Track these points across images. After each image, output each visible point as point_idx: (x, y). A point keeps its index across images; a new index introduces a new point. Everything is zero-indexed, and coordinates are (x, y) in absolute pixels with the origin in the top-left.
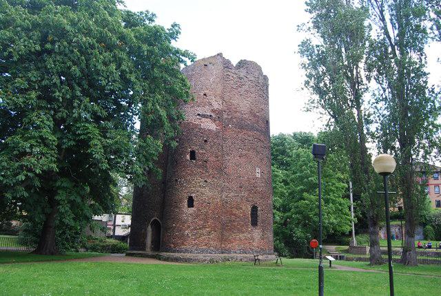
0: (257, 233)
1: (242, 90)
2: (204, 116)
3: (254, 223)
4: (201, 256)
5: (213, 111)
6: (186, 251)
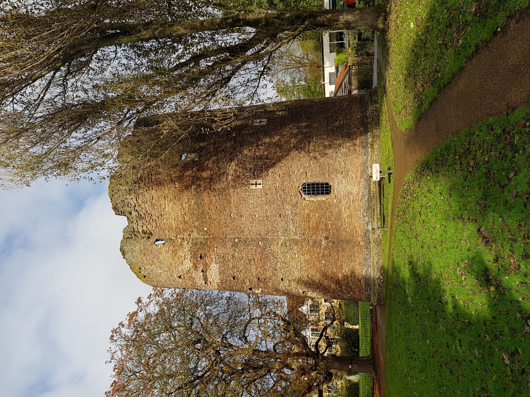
0: (340, 186)
2: (206, 279)
3: (324, 189)
5: (196, 268)
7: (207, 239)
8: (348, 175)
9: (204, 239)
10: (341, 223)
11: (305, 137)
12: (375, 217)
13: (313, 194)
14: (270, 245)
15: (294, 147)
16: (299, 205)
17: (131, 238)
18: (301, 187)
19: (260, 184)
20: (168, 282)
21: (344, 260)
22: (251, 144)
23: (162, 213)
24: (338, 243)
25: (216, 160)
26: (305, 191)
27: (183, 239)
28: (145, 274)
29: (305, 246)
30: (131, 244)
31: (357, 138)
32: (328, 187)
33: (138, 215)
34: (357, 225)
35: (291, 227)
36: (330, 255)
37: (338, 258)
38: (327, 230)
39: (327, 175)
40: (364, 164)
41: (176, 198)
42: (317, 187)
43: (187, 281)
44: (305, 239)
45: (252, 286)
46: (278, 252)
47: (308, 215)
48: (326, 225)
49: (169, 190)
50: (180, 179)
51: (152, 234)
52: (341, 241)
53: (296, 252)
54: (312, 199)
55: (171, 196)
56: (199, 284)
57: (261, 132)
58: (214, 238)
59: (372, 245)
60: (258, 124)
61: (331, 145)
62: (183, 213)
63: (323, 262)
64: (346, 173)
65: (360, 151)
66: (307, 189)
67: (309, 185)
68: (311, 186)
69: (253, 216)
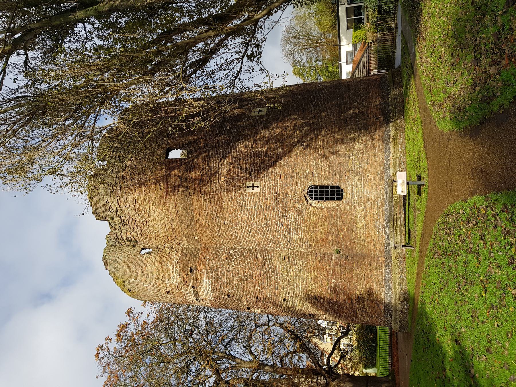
1: (140, 220)
2: (197, 295)
3: (334, 193)
5: (185, 283)
7: (199, 249)
8: (364, 176)
9: (195, 249)
10: (356, 234)
11: (313, 130)
12: (398, 229)
13: (322, 199)
14: (271, 259)
15: (299, 142)
16: (304, 212)
17: (116, 246)
18: (306, 191)
19: (258, 187)
20: (155, 297)
21: (359, 280)
22: (249, 136)
23: (147, 219)
24: (352, 258)
25: (207, 157)
26: (310, 195)
27: (172, 248)
28: (130, 287)
29: (311, 261)
30: (115, 253)
31: (376, 131)
32: (339, 191)
33: (120, 221)
34: (375, 237)
35: (295, 237)
36: (341, 273)
37: (352, 277)
38: (338, 242)
39: (338, 176)
40: (384, 163)
41: (162, 202)
42: (326, 191)
43: (176, 297)
44: (311, 252)
45: (249, 306)
46: (279, 268)
47: (315, 224)
48: (336, 236)
49: (154, 192)
50: (166, 179)
51: (137, 242)
52: (356, 256)
53: (301, 268)
54: (320, 205)
55: (156, 200)
56: (190, 300)
57: (259, 124)
58: (207, 248)
59: (394, 261)
60: (257, 114)
61: (343, 139)
62: (170, 219)
63: (333, 281)
64: (361, 174)
65: (379, 146)
66: (313, 193)
67: (316, 188)
68: (319, 190)
69: (250, 224)
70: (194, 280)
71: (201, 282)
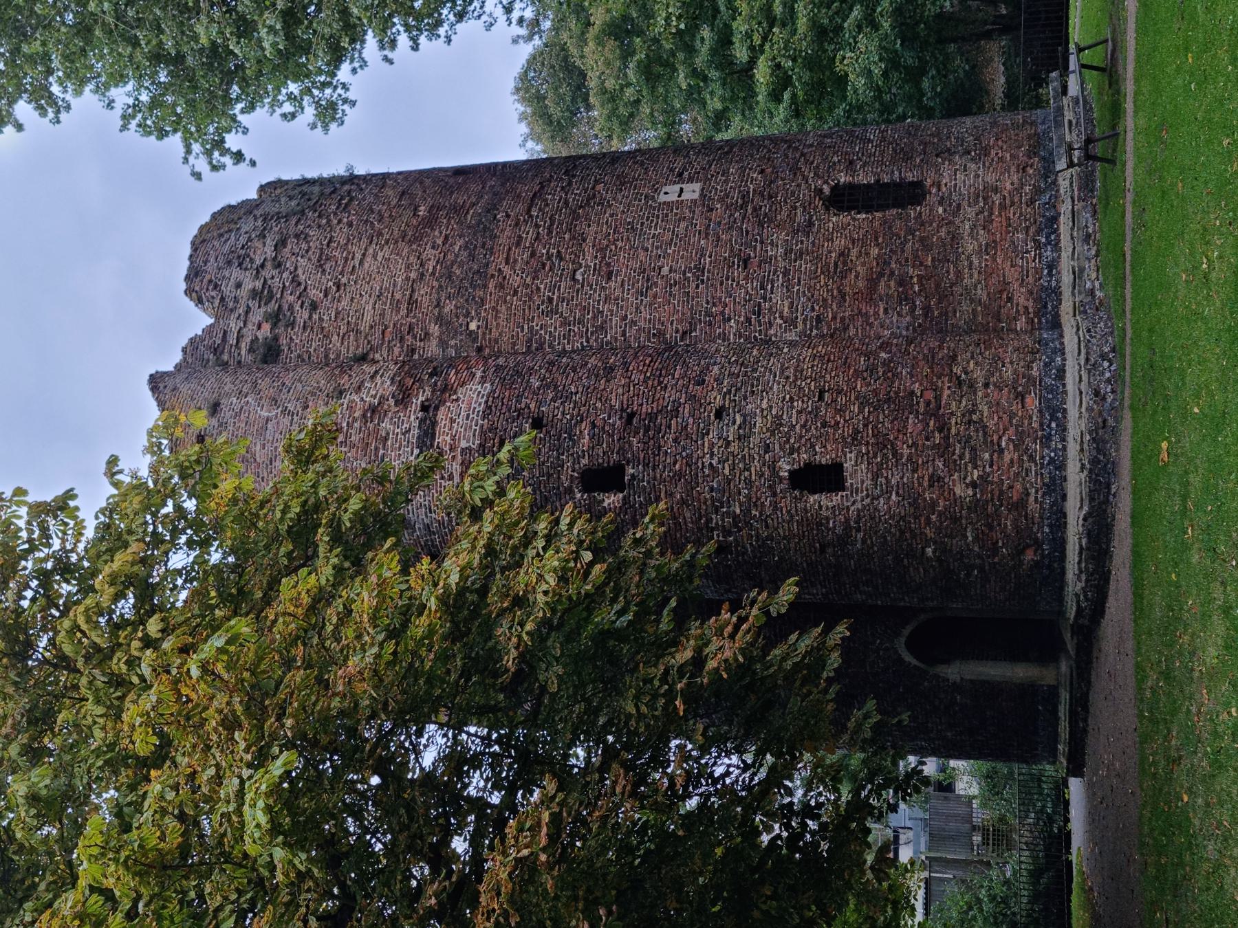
4: (1077, 423)
5: (403, 398)
6: (1055, 488)
23: (344, 280)
70: (433, 391)
71: (455, 393)
